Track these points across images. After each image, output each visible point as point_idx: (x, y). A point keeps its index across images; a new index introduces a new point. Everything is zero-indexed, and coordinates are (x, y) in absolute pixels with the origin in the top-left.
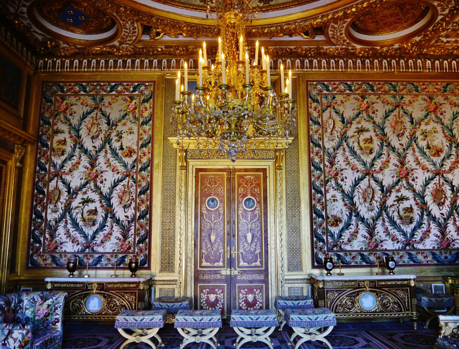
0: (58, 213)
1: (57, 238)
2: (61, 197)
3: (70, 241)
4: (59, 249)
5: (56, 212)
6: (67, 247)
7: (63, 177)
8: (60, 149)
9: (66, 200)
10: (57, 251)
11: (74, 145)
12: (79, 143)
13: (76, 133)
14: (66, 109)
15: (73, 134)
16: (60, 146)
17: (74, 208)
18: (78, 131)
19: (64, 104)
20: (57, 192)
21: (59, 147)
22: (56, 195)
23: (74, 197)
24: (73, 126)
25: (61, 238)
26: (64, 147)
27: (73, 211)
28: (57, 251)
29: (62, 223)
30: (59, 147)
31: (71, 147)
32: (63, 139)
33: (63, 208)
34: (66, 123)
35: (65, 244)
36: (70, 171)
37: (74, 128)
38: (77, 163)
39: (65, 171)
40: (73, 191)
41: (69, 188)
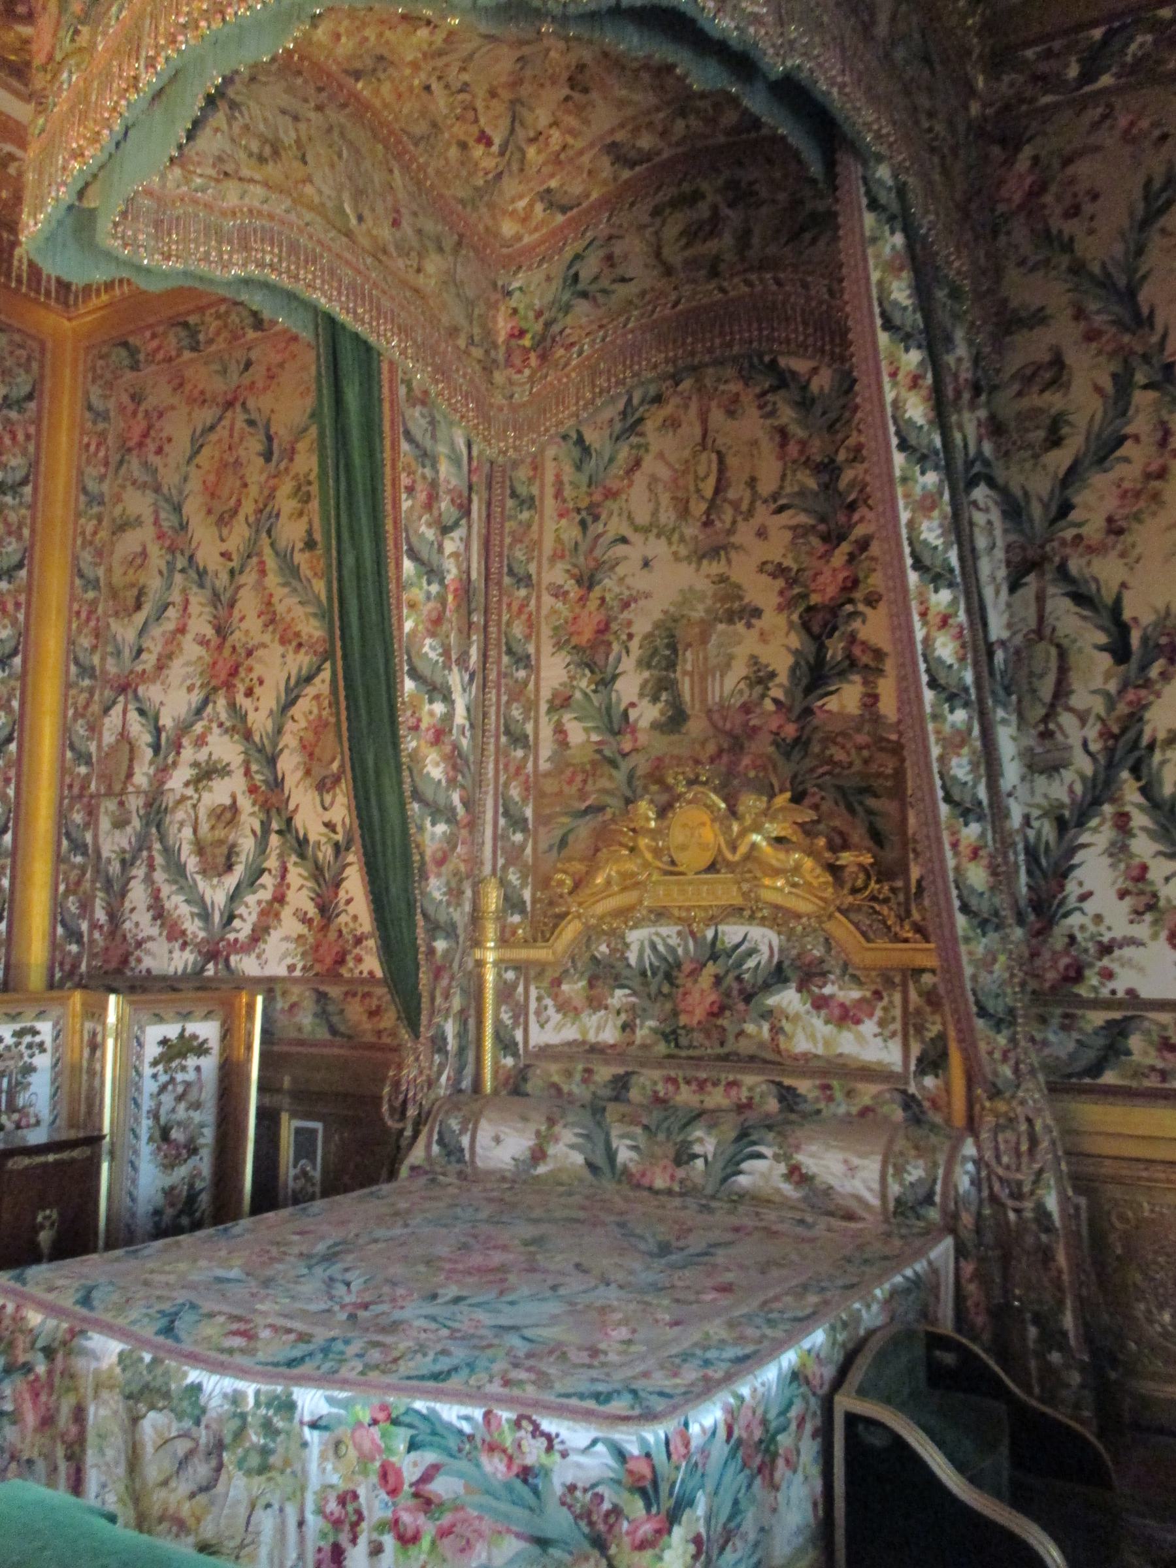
0: (1068, 775)
1: (1075, 920)
2: (1076, 682)
3: (1155, 936)
4: (1094, 981)
5: (1052, 769)
6: (1141, 970)
7: (1074, 566)
8: (1036, 412)
9: (1107, 695)
10: (1083, 991)
11: (1115, 376)
12: (1146, 358)
13: (1117, 309)
14: (1040, 189)
15: (1099, 320)
16: (1034, 400)
17: (1162, 735)
18: (1130, 295)
19: (1023, 162)
20: (1046, 656)
21: (1025, 403)
22: (1041, 676)
23: (1154, 672)
24: (1096, 269)
25: (1098, 918)
26: (1054, 401)
27: (1157, 757)
28: (1083, 991)
29: (1095, 830)
30: (1025, 403)
31: (1098, 389)
32: (1047, 357)
33: (1094, 747)
34: (1047, 262)
35: (1128, 952)
36: (1115, 529)
37: (1105, 283)
38: (1148, 476)
39: (1084, 531)
40: (1145, 640)
41: (1119, 629)
